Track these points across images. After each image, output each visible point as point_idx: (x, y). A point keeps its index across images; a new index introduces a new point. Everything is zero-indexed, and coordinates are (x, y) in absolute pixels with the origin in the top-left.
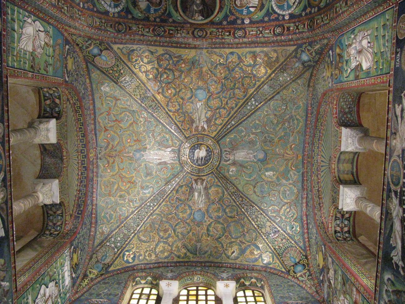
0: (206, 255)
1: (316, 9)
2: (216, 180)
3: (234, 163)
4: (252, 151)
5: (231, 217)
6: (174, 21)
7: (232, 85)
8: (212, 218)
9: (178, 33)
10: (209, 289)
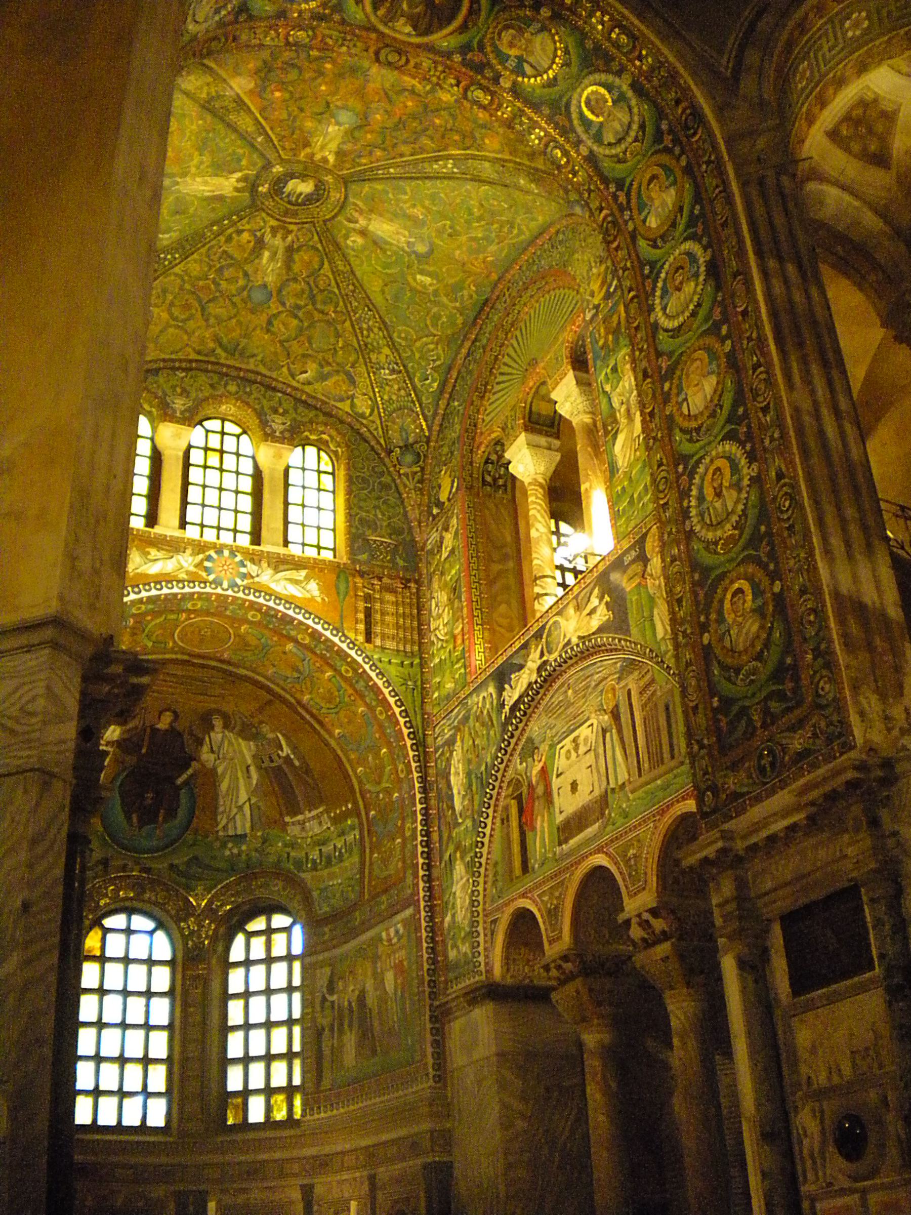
0: (252, 360)
1: (631, 226)
2: (316, 238)
3: (363, 233)
4: (407, 233)
5: (322, 312)
6: (343, 22)
7: (419, 128)
8: (284, 304)
9: (343, 45)
10: (245, 432)
